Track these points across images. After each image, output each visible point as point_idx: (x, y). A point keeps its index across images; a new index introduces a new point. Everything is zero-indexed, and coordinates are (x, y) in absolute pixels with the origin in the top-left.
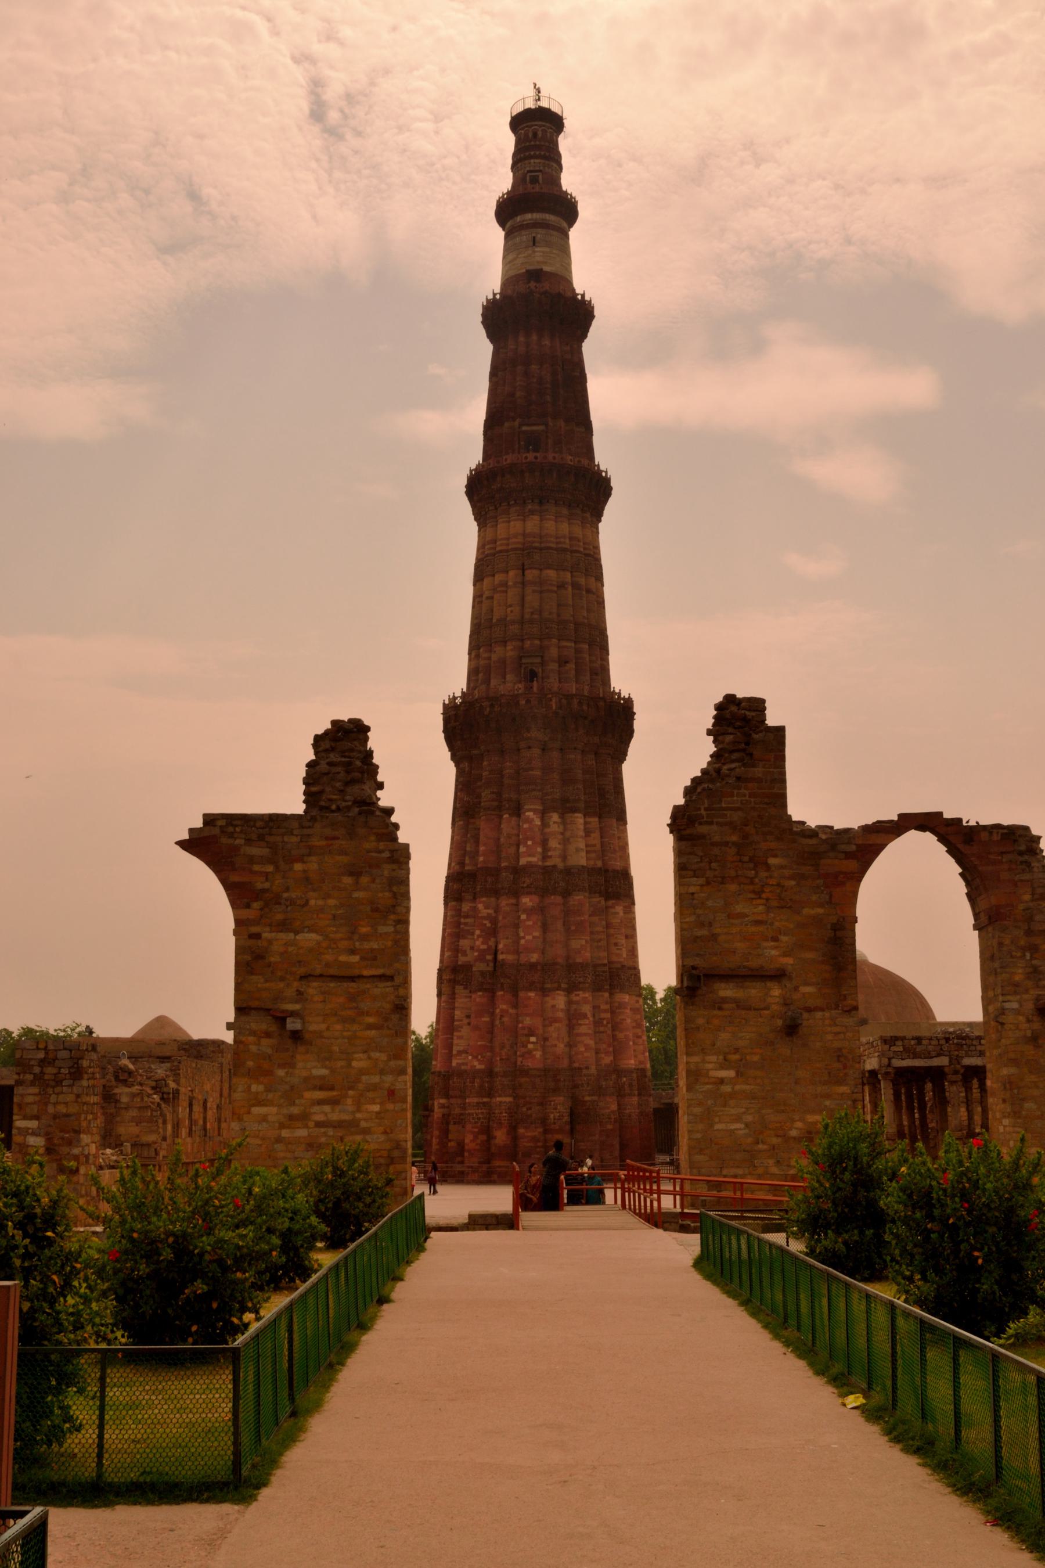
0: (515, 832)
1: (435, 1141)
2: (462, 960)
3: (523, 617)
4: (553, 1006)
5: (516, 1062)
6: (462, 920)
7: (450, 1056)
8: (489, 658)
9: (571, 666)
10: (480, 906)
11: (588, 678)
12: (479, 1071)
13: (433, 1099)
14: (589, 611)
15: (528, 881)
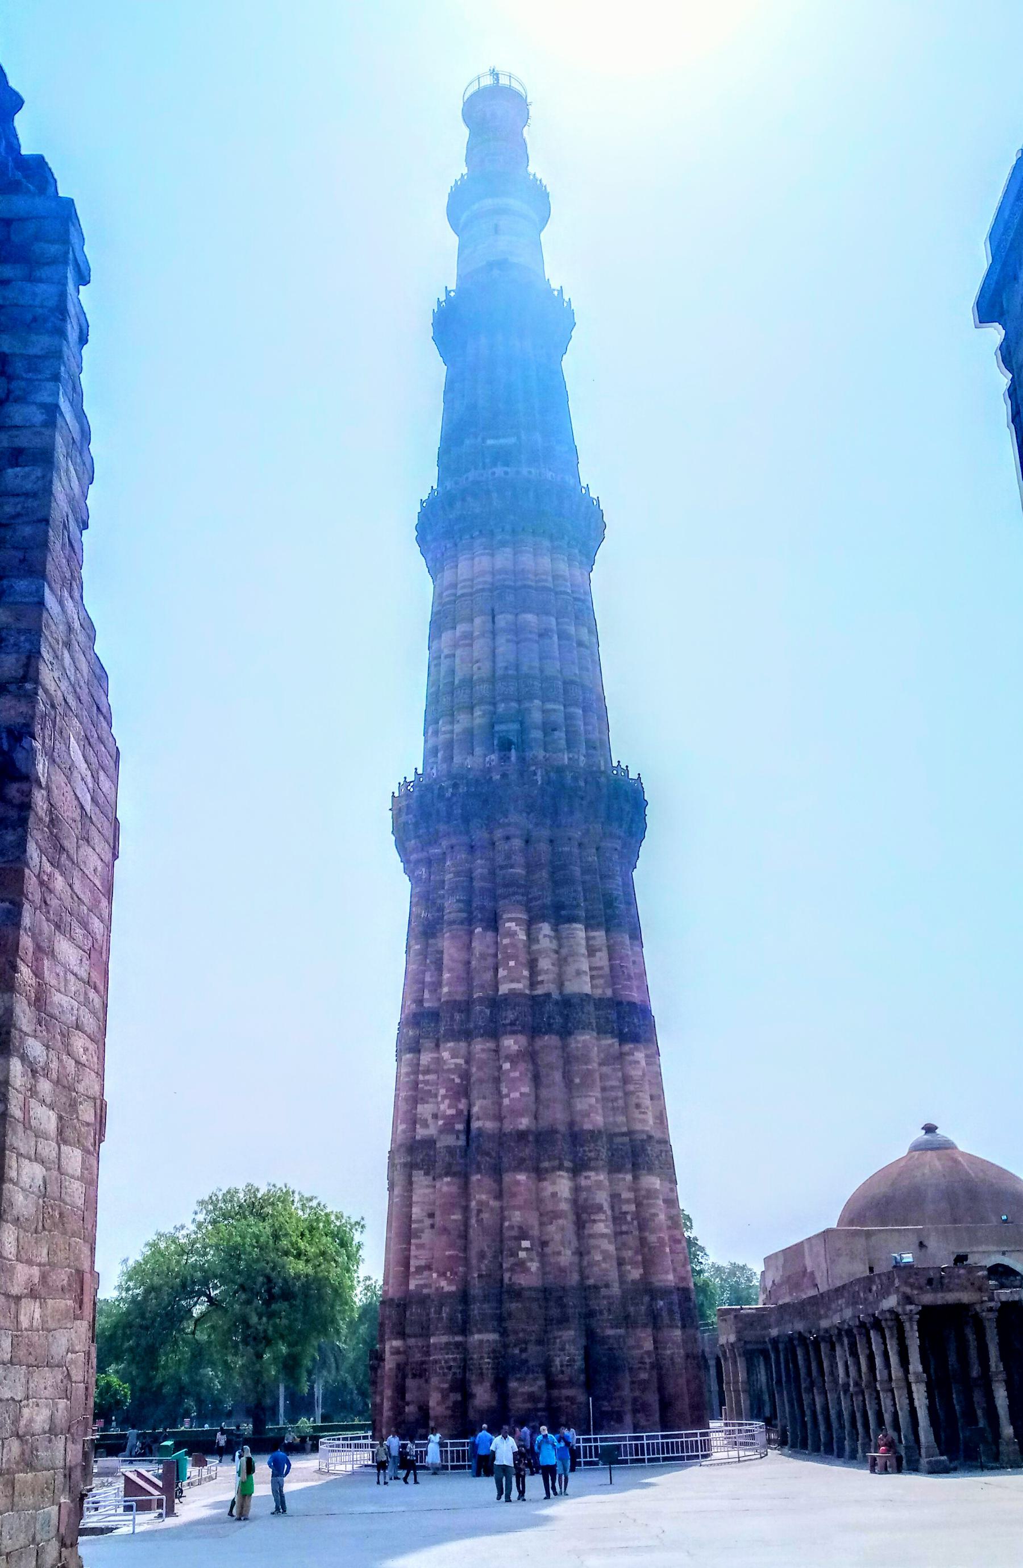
0: (492, 951)
1: (387, 1405)
2: (421, 1132)
3: (493, 676)
4: (554, 1195)
5: (502, 1280)
6: (421, 1077)
7: (406, 1275)
8: (452, 732)
9: (560, 735)
10: (446, 1055)
11: (583, 751)
12: (450, 1294)
13: (382, 1341)
14: (581, 669)
15: (511, 1015)
